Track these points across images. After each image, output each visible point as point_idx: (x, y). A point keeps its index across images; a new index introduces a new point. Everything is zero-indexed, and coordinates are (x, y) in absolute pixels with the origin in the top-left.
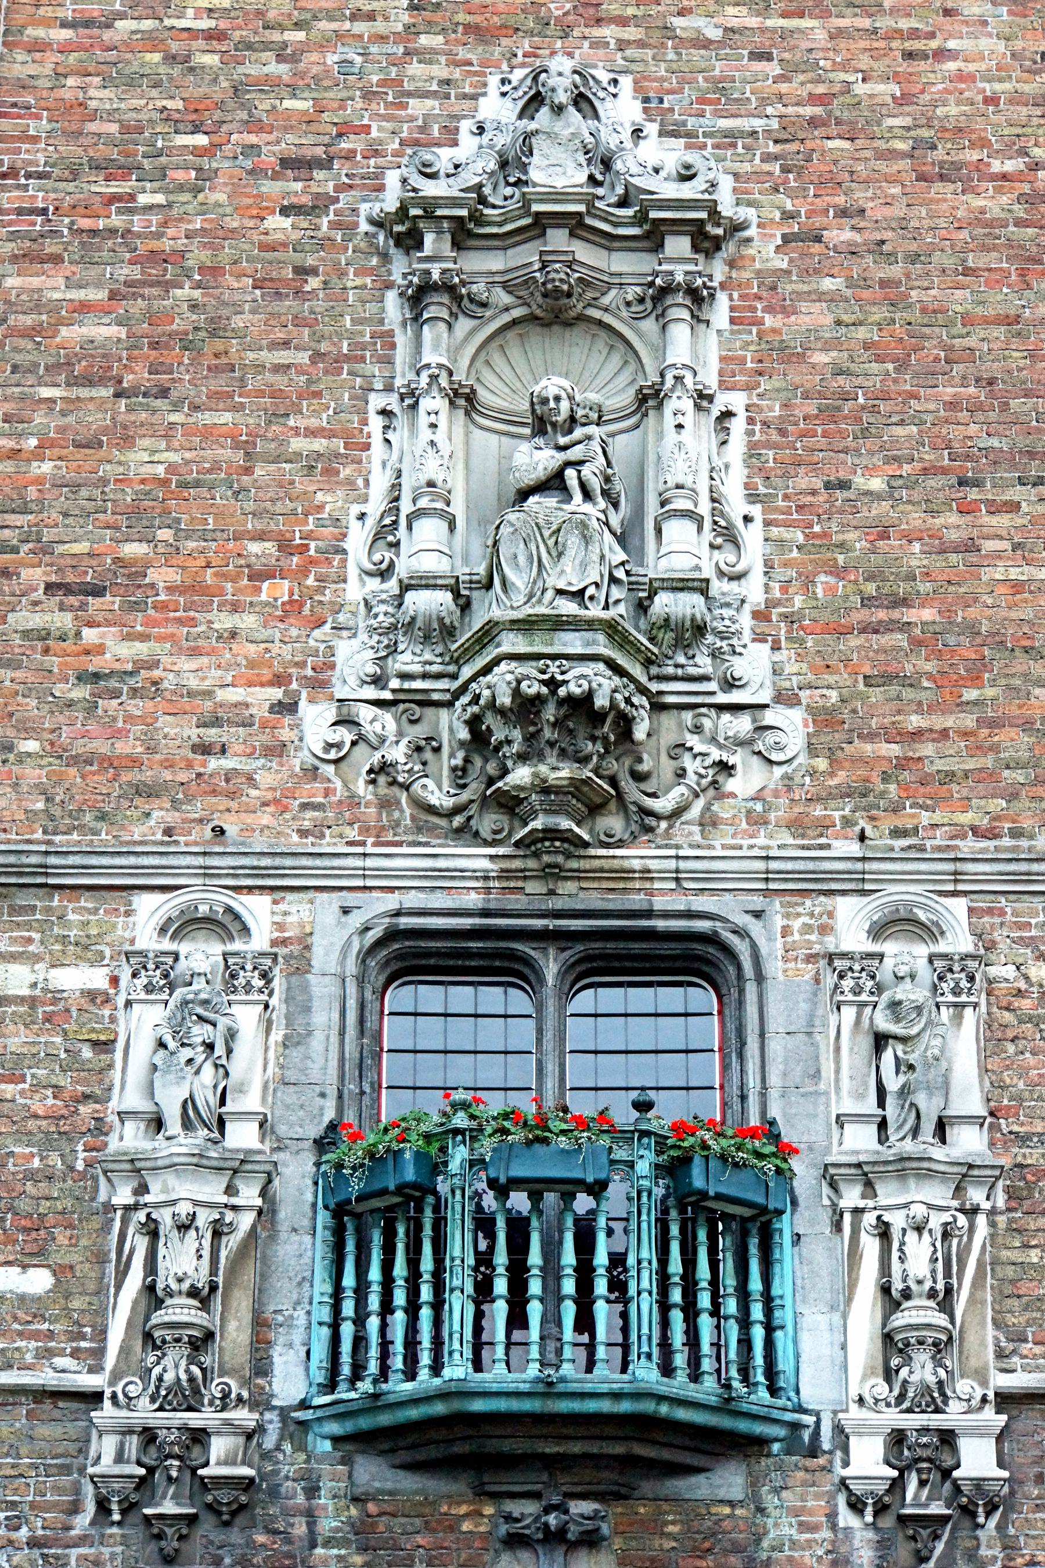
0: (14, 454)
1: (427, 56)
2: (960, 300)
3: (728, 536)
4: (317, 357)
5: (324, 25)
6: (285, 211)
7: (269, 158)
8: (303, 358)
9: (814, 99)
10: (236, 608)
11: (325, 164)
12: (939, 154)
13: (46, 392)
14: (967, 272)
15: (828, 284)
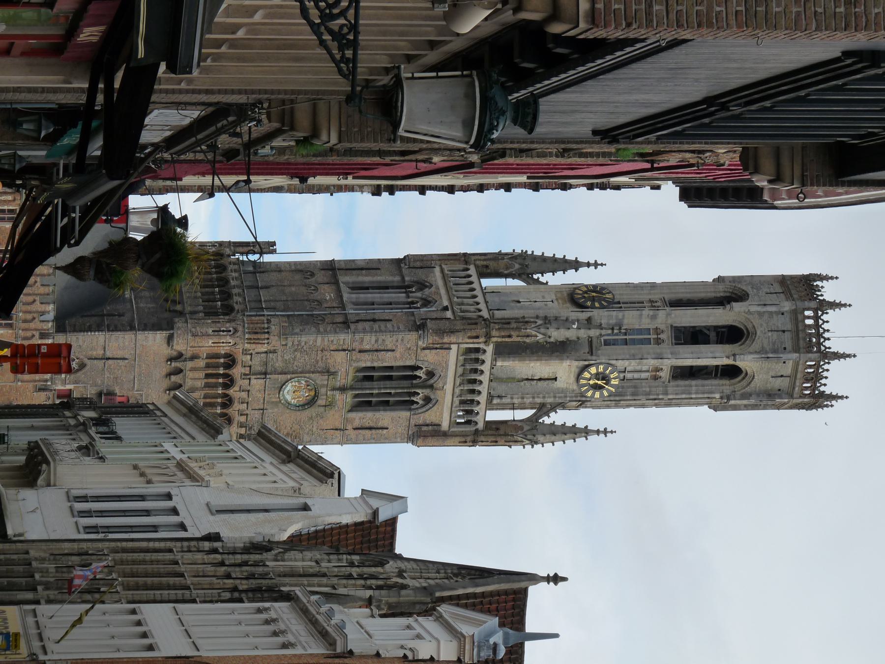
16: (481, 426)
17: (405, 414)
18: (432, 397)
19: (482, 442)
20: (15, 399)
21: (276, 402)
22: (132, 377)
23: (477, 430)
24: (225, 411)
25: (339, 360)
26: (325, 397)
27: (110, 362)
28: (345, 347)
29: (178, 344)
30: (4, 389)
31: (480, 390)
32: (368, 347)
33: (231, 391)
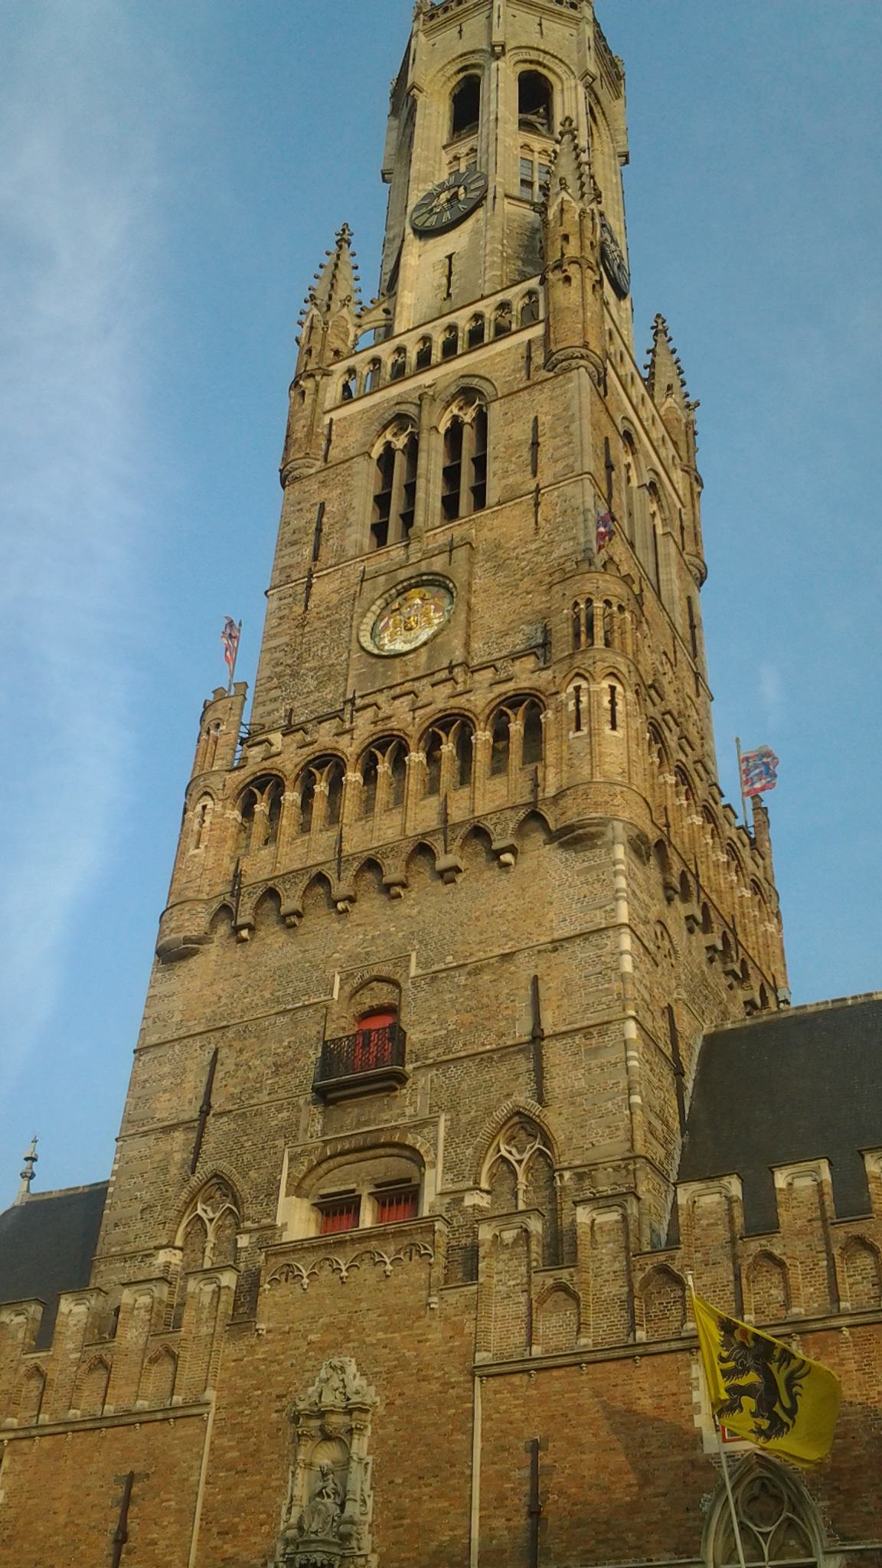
0: (213, 1494)
1: (309, 1358)
2: (424, 1419)
3: (364, 1502)
4: (280, 1455)
5: (289, 1352)
6: (276, 1411)
7: (274, 1396)
8: (276, 1456)
9: (397, 1359)
10: (256, 1535)
11: (285, 1396)
12: (423, 1373)
13: (221, 1474)
14: (427, 1410)
15: (395, 1418)
16: (533, 283)
17: (495, 413)
18: (453, 389)
19: (563, 255)
20: (278, 1405)
21: (430, 651)
22: (282, 1020)
23: (543, 281)
24: (412, 743)
25: (336, 585)
26: (423, 563)
27: (218, 1102)
28: (301, 589)
29: (180, 928)
30: (235, 1454)
31: (440, 329)
32: (308, 551)
33: (349, 751)
